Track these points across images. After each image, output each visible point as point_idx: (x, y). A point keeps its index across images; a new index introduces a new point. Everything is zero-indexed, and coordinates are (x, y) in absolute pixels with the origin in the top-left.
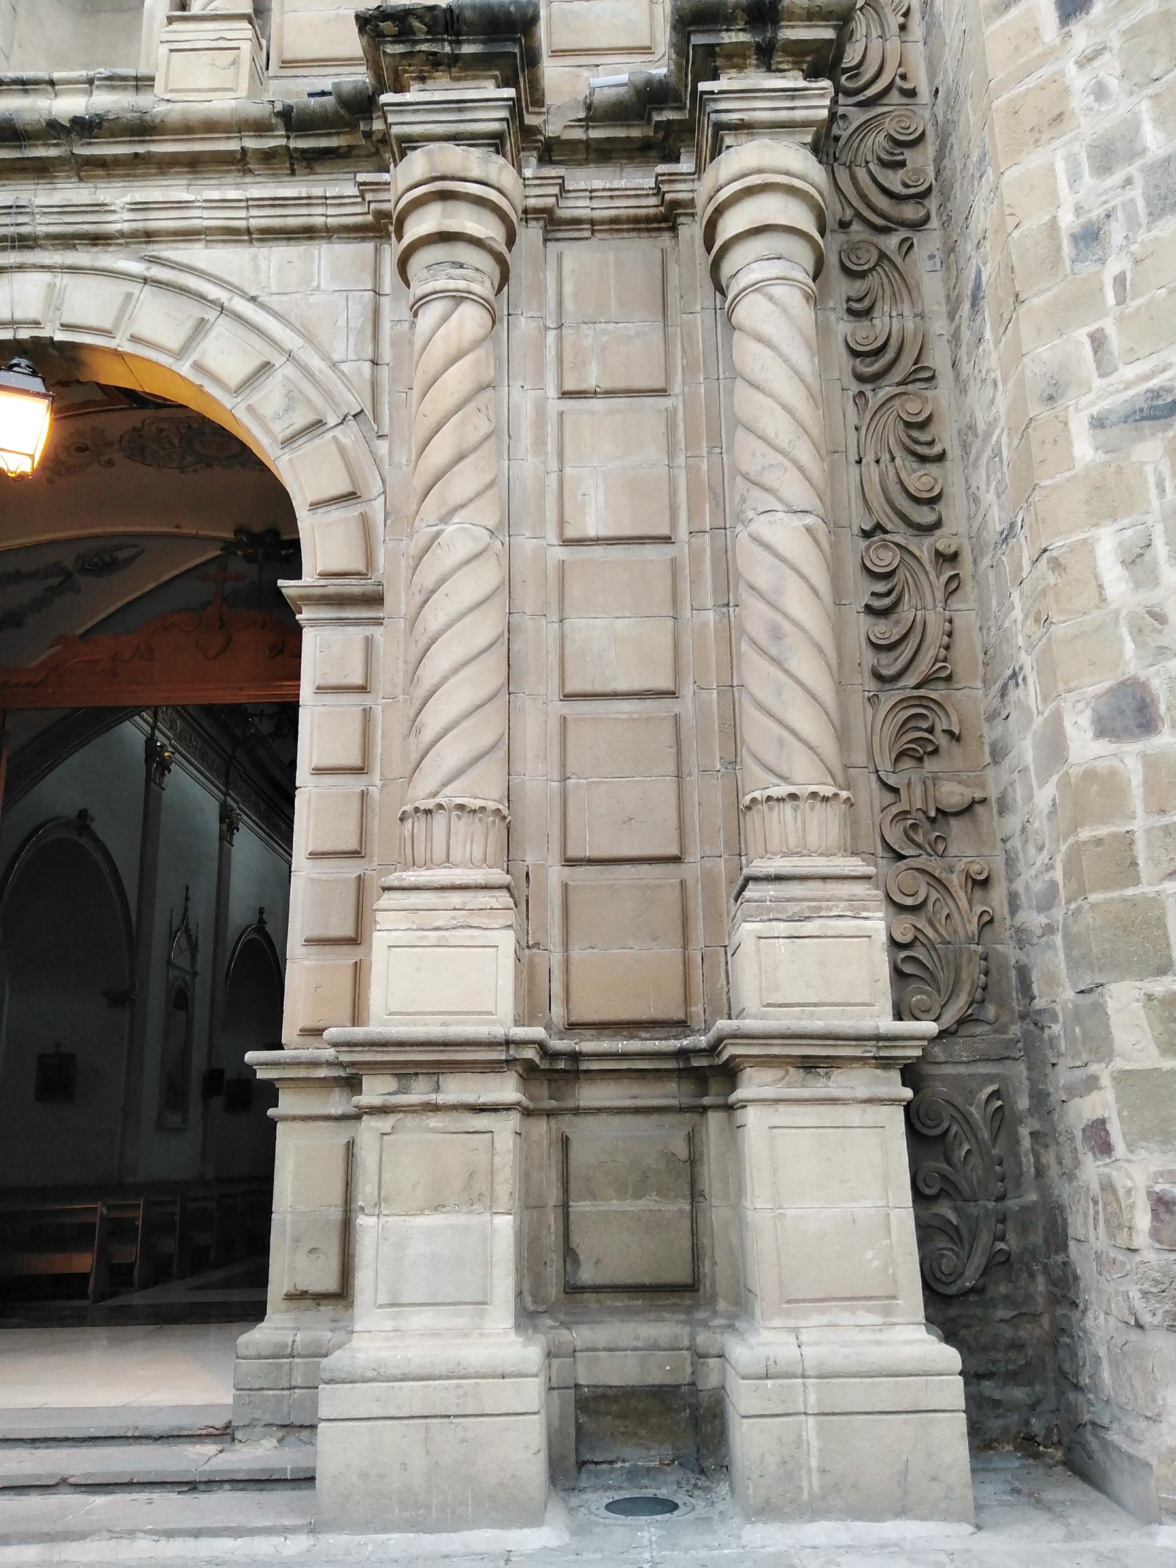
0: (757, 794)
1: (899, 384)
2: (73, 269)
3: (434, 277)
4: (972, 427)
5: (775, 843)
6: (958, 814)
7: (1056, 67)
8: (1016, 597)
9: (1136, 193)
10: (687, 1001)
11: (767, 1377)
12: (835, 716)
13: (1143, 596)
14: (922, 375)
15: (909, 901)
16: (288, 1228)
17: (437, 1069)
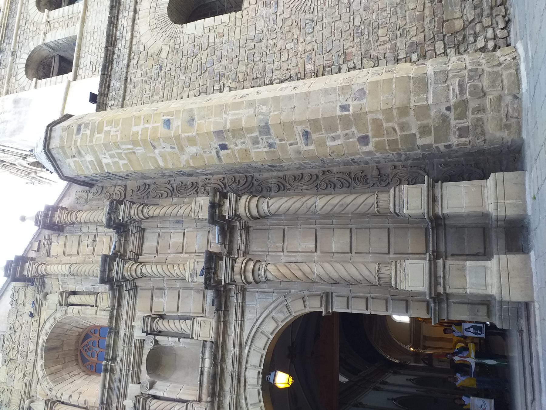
0: (376, 210)
1: (286, 182)
2: (247, 363)
3: (261, 274)
4: (298, 168)
5: (387, 206)
6: (380, 172)
7: (236, 150)
8: (336, 160)
9: (264, 137)
10: (421, 228)
11: (498, 210)
12: (360, 194)
13: (341, 137)
14: (285, 177)
15: (399, 181)
16: (472, 317)
17: (436, 276)
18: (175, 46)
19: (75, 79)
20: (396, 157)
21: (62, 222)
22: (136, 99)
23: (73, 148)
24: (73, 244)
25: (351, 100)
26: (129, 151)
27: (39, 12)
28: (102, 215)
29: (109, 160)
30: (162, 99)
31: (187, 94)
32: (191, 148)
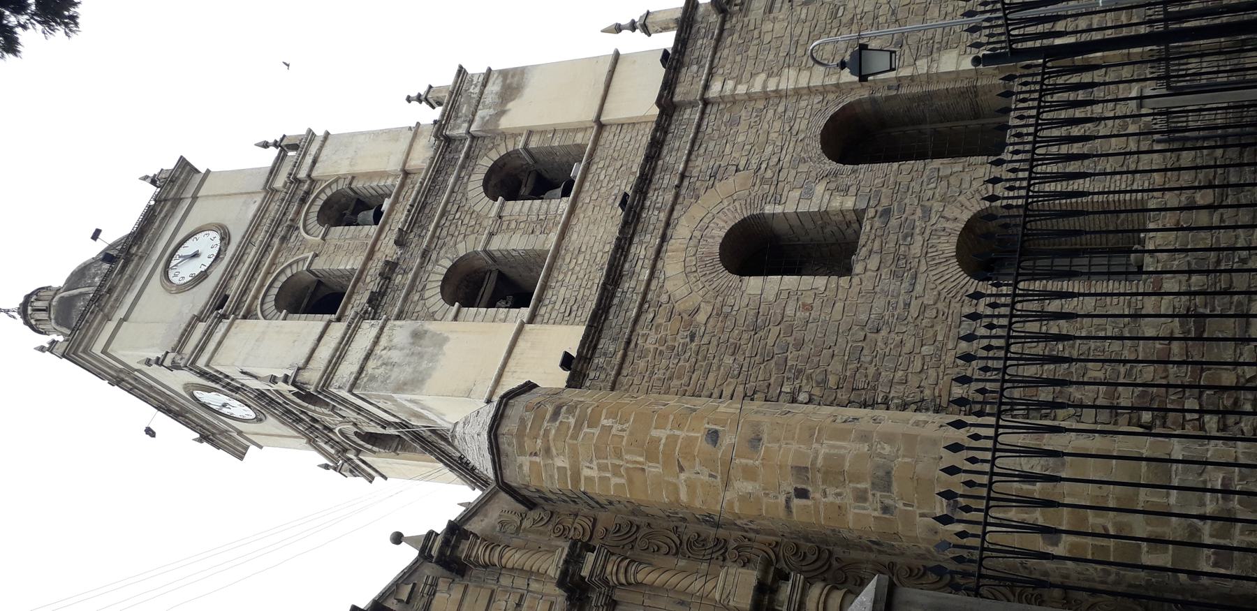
9: (878, 494)
18: (724, 307)
19: (531, 320)
20: (1101, 574)
21: (472, 559)
22: (640, 377)
23: (539, 441)
24: (478, 603)
25: (1039, 468)
26: (634, 466)
27: (487, 199)
28: (550, 561)
29: (594, 473)
30: (686, 388)
31: (732, 388)
32: (745, 483)
